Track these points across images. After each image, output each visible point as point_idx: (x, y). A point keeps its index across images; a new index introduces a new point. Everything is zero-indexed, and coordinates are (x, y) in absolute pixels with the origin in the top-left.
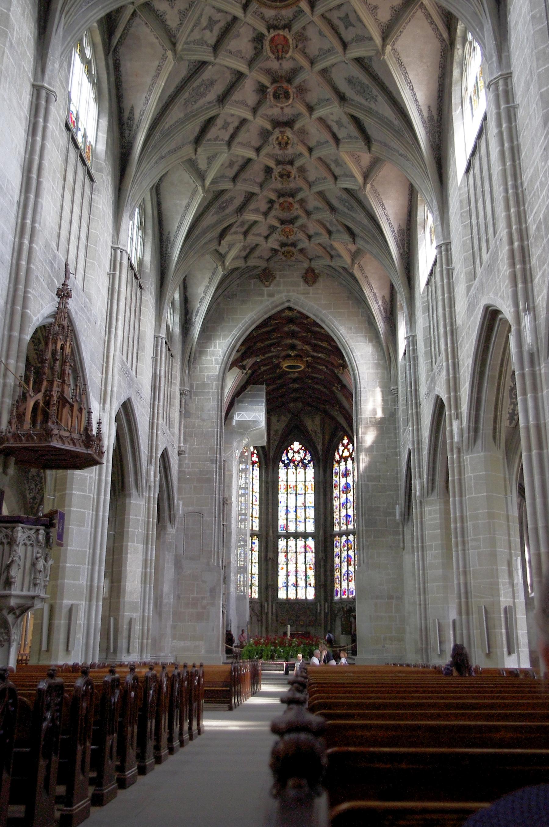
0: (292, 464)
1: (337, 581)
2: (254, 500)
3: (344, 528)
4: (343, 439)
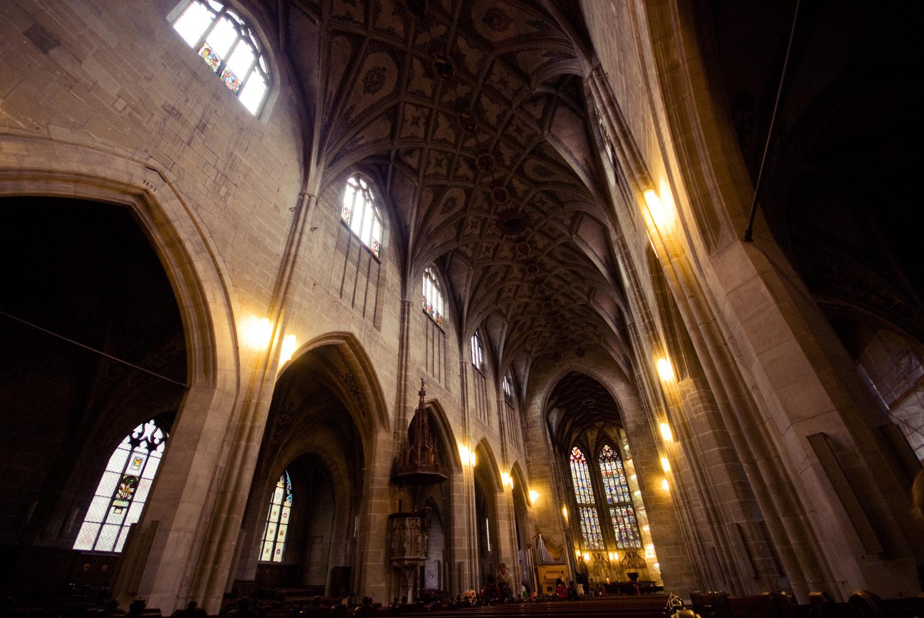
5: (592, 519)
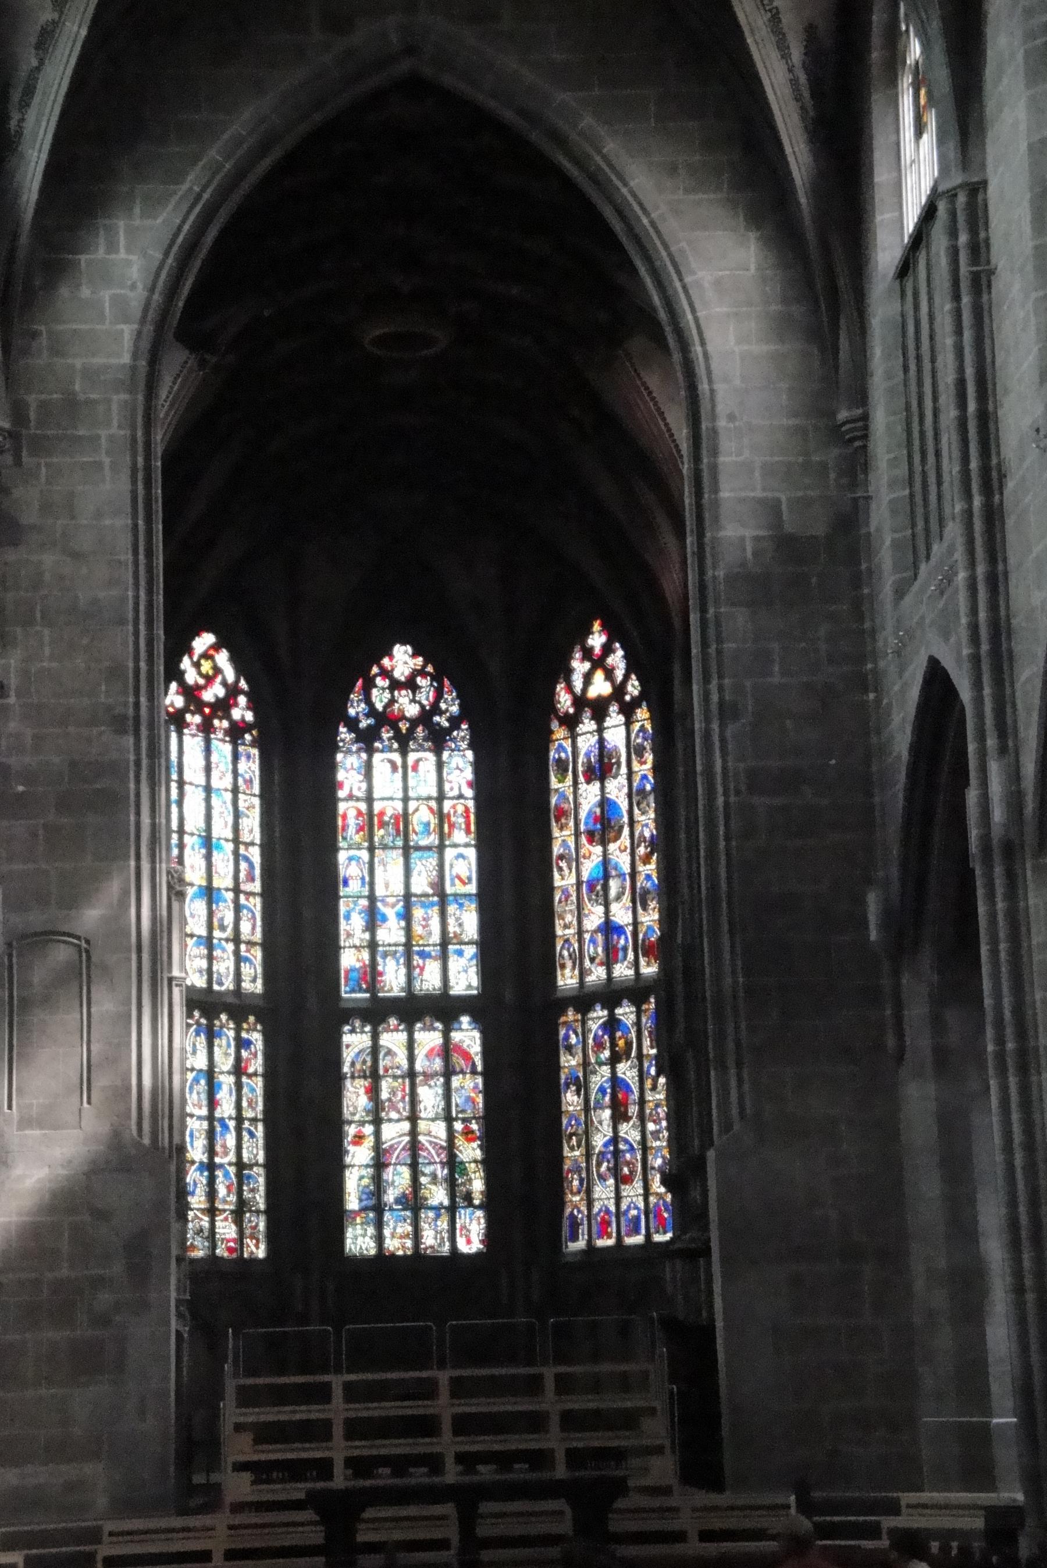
0: (386, 734)
1: (576, 1183)
2: (242, 875)
3: (597, 974)
4: (589, 632)
5: (227, 1081)
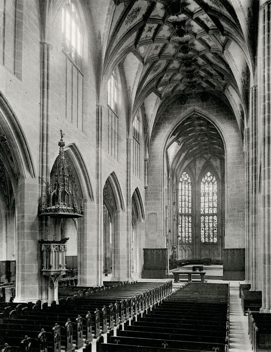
0: (207, 183)
